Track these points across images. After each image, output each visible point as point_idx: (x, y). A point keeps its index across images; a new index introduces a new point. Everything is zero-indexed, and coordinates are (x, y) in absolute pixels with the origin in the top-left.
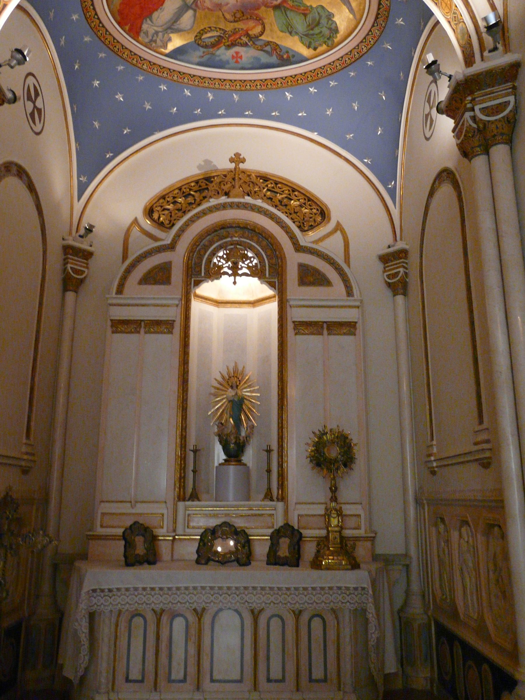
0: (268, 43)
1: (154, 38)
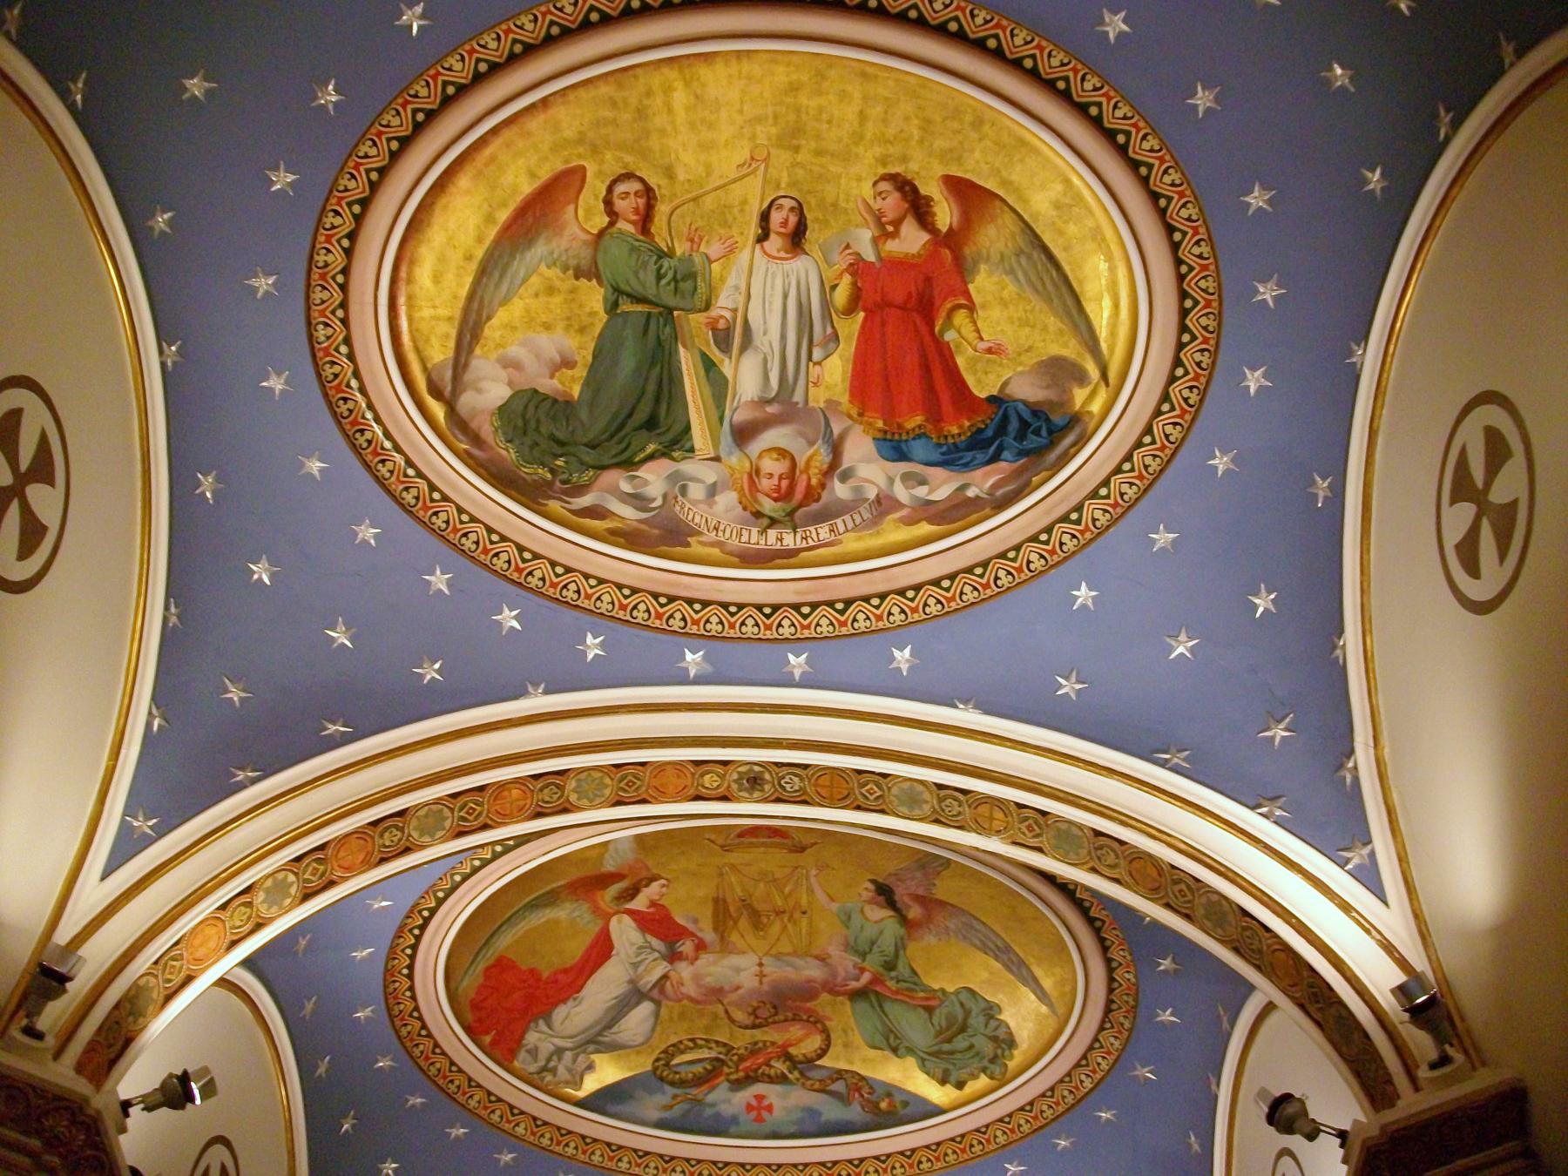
0: (840, 1074)
1: (552, 1064)
